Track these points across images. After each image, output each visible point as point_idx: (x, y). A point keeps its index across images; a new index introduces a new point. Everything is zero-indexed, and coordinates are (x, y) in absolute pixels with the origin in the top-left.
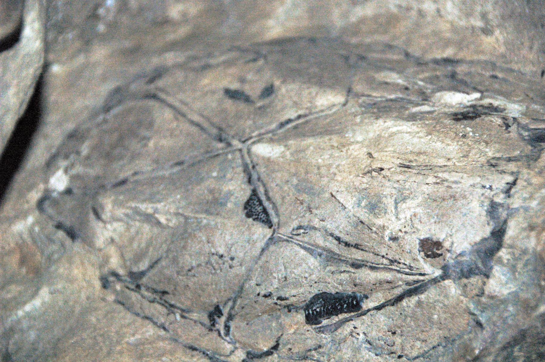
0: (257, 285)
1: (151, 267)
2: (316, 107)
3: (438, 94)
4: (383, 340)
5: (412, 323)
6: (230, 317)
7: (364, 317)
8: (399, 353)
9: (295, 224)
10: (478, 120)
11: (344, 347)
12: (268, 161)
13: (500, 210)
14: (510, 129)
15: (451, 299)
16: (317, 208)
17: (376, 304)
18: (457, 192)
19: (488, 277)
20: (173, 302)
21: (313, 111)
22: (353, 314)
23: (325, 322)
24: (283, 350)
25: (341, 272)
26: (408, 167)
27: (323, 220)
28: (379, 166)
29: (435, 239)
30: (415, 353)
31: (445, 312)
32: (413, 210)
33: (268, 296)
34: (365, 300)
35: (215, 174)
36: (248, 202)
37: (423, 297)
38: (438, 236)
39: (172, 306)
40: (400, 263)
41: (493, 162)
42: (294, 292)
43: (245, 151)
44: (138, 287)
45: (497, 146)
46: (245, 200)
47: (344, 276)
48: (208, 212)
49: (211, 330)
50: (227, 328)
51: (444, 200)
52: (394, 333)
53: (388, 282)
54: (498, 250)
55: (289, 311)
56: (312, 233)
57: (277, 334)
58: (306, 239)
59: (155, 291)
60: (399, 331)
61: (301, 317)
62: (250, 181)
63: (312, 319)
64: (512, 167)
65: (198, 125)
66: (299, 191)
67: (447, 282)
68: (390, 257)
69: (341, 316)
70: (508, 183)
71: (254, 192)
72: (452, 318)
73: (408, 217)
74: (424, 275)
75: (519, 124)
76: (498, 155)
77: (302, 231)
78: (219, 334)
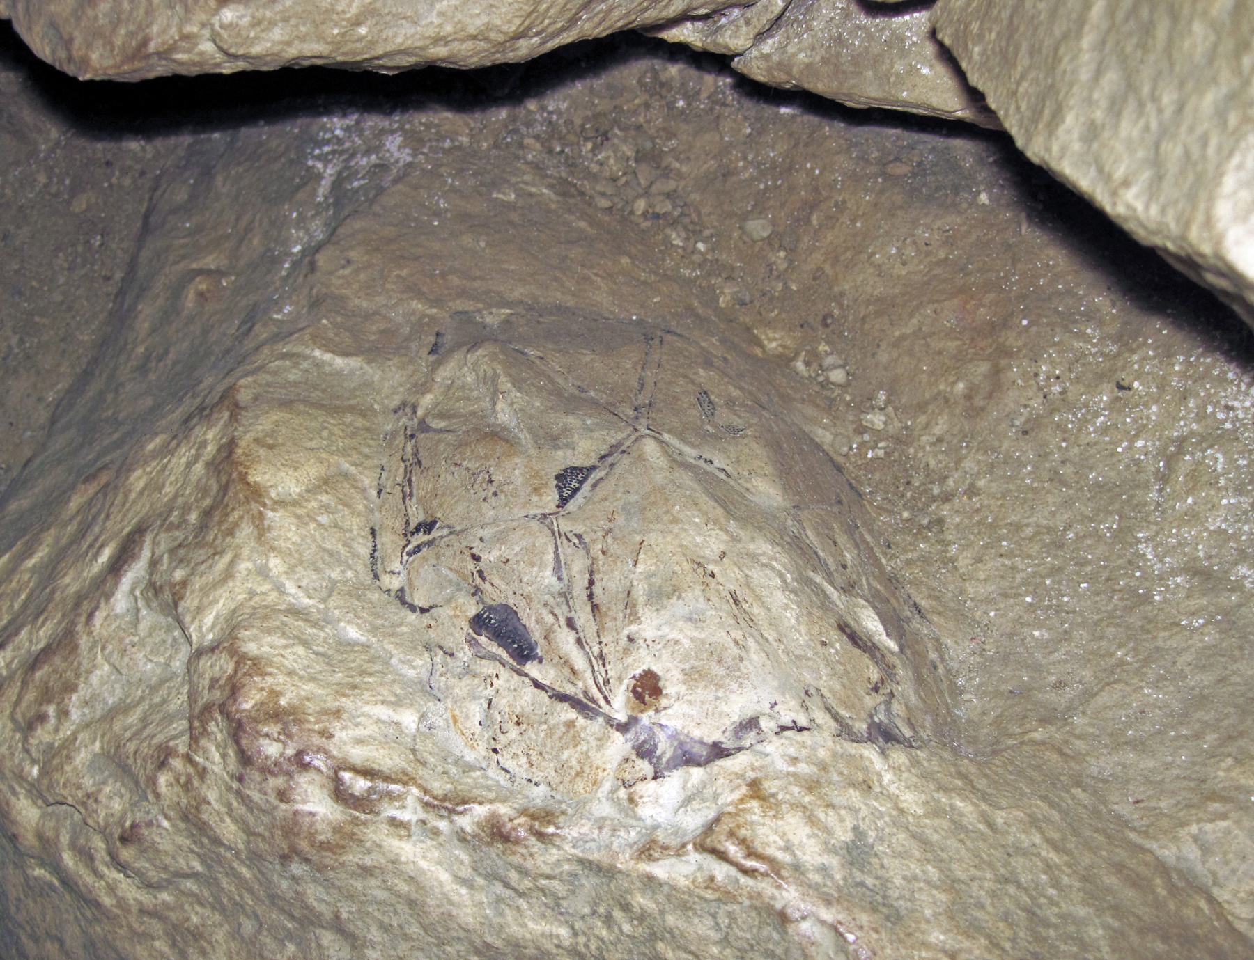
0: (481, 539)
1: (441, 431)
2: (750, 482)
3: (862, 602)
4: (502, 717)
5: (542, 734)
6: (430, 543)
7: (515, 676)
8: (498, 747)
9: (579, 529)
10: (858, 652)
11: (467, 680)
12: (641, 458)
13: (753, 734)
14: (874, 694)
15: (599, 755)
16: (615, 539)
17: (539, 678)
18: (739, 670)
19: (655, 778)
20: (414, 479)
21: (741, 481)
22: (511, 661)
23: (483, 639)
24: (427, 619)
25: (552, 613)
26: (736, 602)
27: (604, 552)
28: (715, 571)
29: (661, 684)
30: (510, 764)
31: (579, 762)
32: (681, 637)
33: (476, 558)
34: (535, 662)
35: (589, 422)
36: (575, 468)
37: (581, 721)
38: (668, 684)
39: (410, 481)
40: (604, 665)
41: (812, 691)
42: (497, 581)
43: (637, 434)
44: (412, 436)
45: (838, 687)
46: (578, 464)
47: (549, 619)
48: (536, 437)
49: (405, 535)
50: (418, 549)
51: (719, 662)
52: (518, 724)
53: (573, 671)
54: (699, 765)
55: (474, 594)
56: (582, 552)
57: (439, 600)
58: (569, 551)
59: (415, 454)
60: (524, 726)
61: (473, 611)
62: (602, 458)
63: (478, 622)
64: (821, 717)
65: (642, 385)
66: (623, 509)
67: (617, 737)
68: (605, 651)
69: (503, 654)
70: (794, 722)
71: (593, 468)
72: (577, 774)
73: (671, 637)
74: (608, 702)
75: (888, 704)
76: (826, 692)
77: (576, 541)
78: (404, 547)
